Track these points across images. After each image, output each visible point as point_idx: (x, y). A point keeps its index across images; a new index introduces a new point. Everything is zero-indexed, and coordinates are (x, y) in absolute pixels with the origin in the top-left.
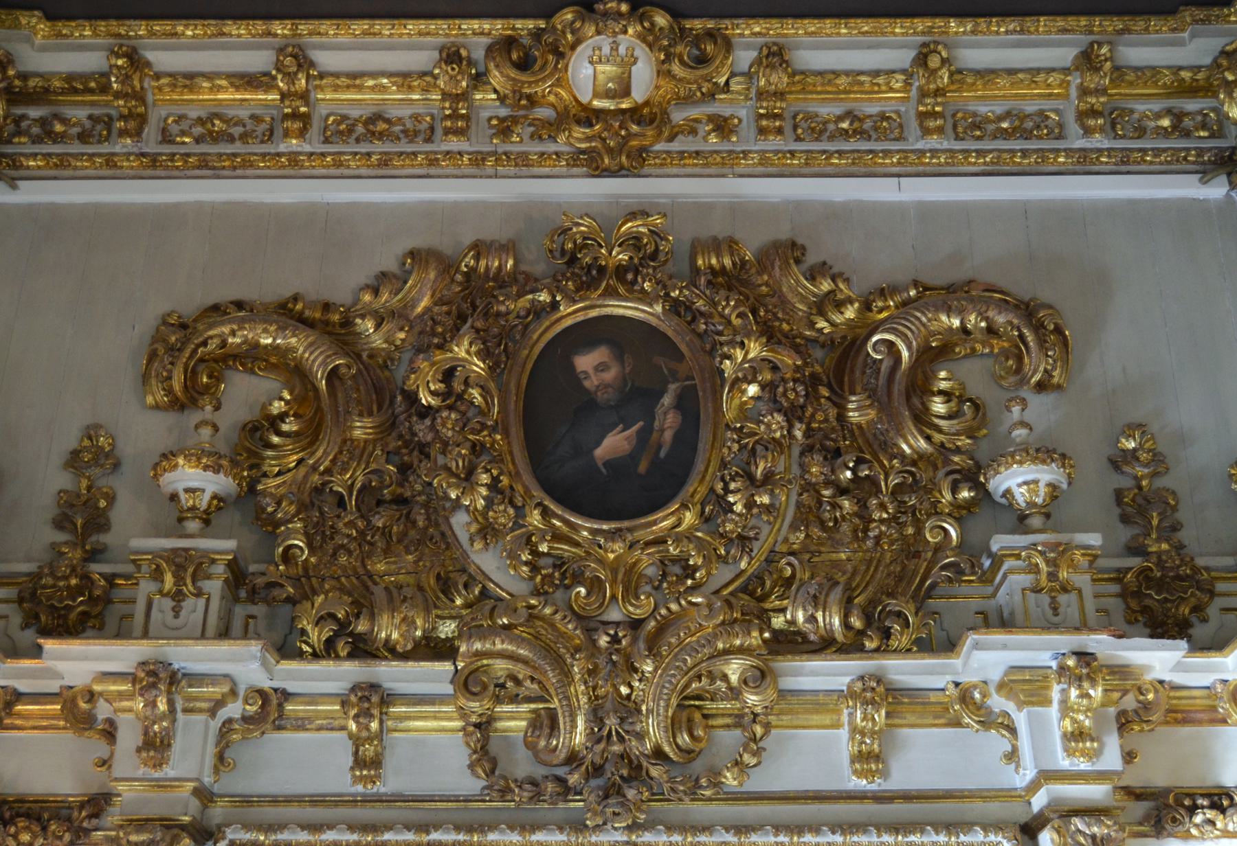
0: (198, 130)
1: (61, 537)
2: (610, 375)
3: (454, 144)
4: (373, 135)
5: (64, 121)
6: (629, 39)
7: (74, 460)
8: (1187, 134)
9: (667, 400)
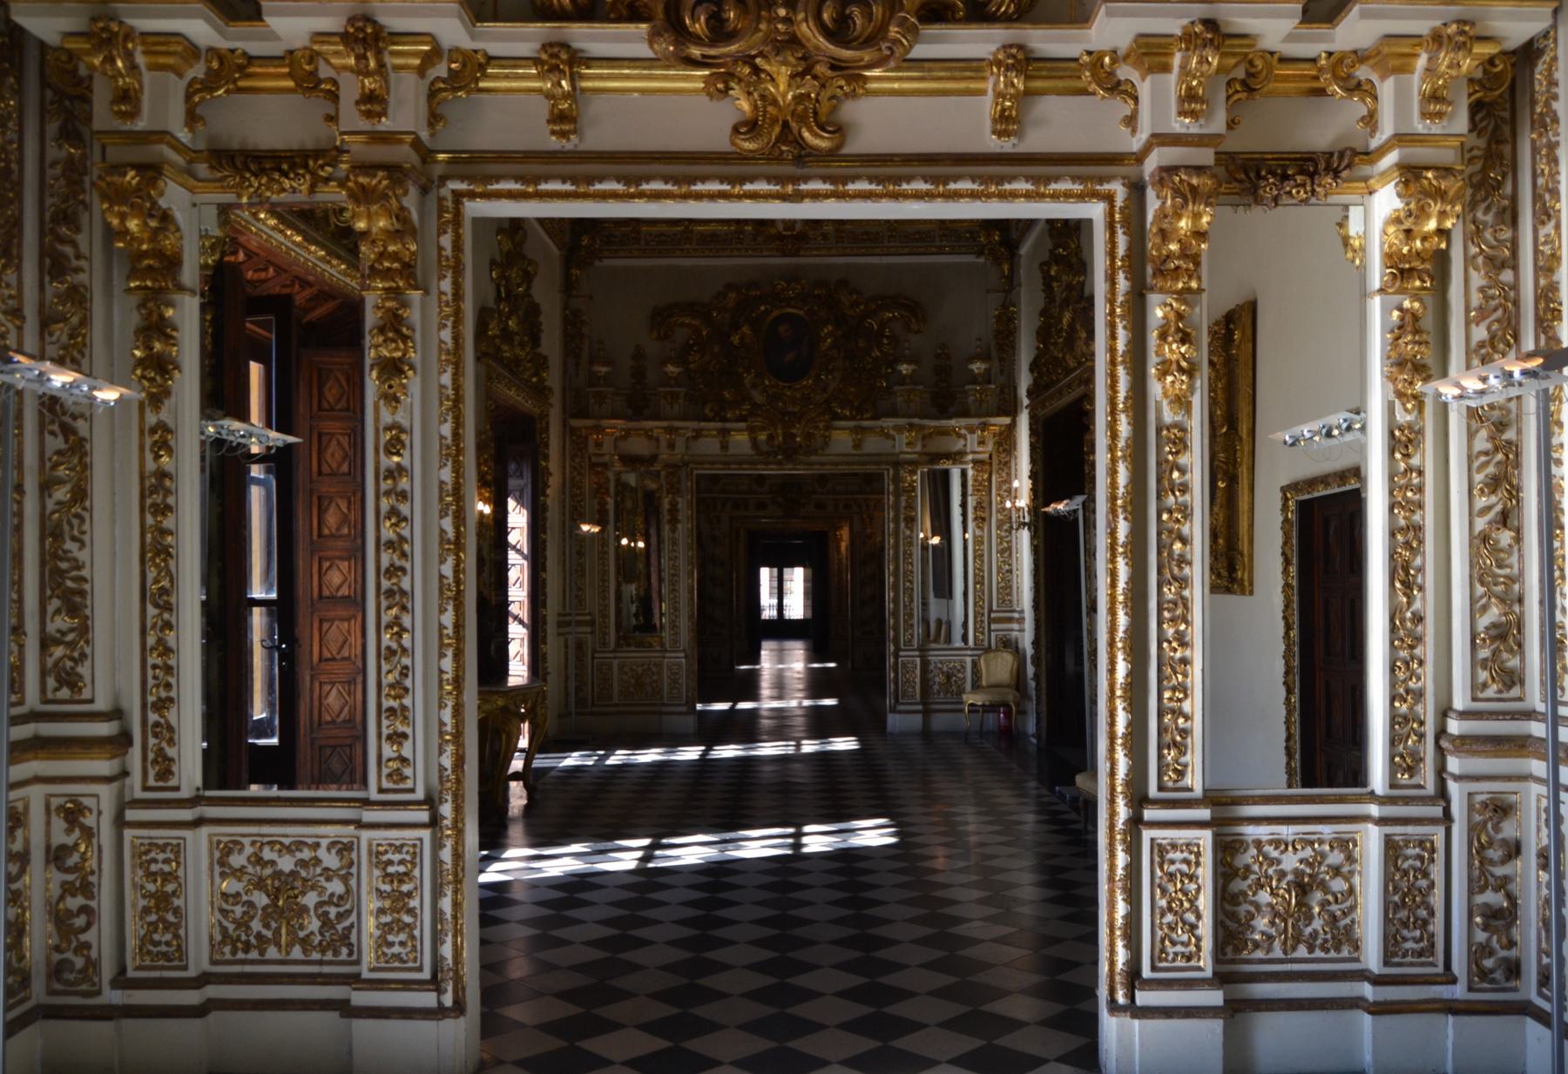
3: (739, 246)
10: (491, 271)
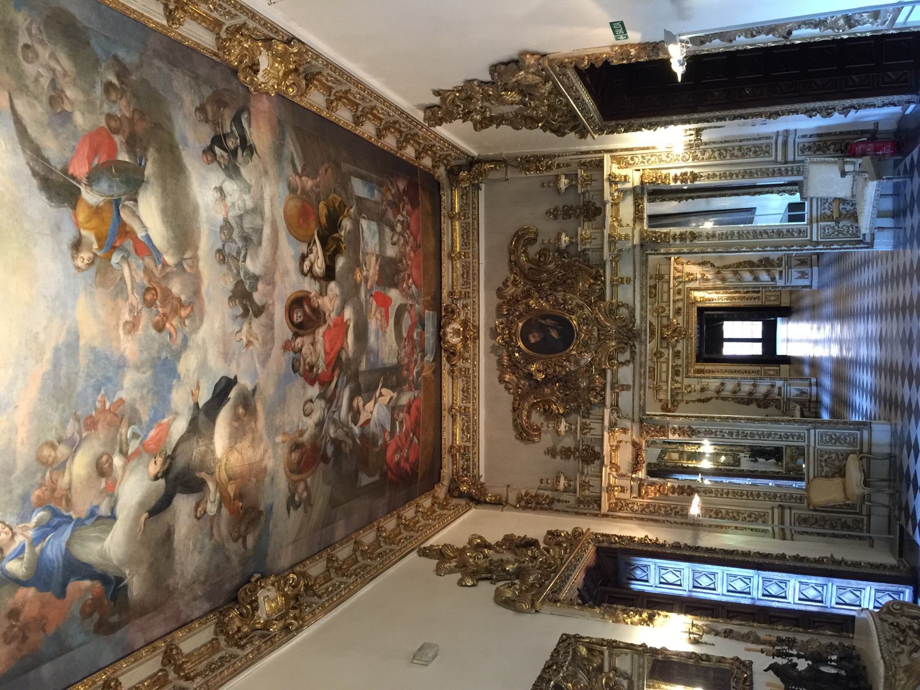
0: (466, 433)
1: (572, 457)
2: (536, 335)
3: (471, 371)
4: (468, 392)
5: (463, 466)
6: (449, 330)
7: (554, 456)
8: (468, 192)
9: (543, 322)
10: (466, 586)
